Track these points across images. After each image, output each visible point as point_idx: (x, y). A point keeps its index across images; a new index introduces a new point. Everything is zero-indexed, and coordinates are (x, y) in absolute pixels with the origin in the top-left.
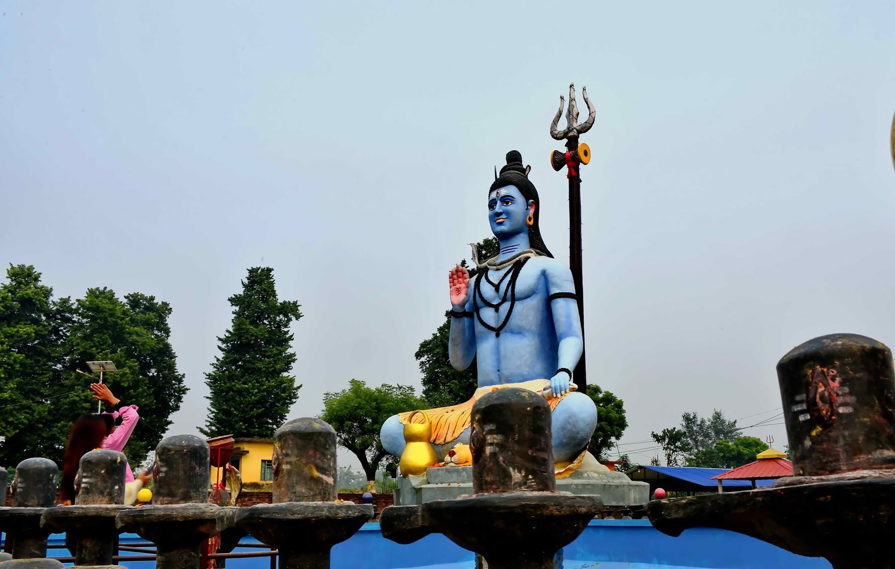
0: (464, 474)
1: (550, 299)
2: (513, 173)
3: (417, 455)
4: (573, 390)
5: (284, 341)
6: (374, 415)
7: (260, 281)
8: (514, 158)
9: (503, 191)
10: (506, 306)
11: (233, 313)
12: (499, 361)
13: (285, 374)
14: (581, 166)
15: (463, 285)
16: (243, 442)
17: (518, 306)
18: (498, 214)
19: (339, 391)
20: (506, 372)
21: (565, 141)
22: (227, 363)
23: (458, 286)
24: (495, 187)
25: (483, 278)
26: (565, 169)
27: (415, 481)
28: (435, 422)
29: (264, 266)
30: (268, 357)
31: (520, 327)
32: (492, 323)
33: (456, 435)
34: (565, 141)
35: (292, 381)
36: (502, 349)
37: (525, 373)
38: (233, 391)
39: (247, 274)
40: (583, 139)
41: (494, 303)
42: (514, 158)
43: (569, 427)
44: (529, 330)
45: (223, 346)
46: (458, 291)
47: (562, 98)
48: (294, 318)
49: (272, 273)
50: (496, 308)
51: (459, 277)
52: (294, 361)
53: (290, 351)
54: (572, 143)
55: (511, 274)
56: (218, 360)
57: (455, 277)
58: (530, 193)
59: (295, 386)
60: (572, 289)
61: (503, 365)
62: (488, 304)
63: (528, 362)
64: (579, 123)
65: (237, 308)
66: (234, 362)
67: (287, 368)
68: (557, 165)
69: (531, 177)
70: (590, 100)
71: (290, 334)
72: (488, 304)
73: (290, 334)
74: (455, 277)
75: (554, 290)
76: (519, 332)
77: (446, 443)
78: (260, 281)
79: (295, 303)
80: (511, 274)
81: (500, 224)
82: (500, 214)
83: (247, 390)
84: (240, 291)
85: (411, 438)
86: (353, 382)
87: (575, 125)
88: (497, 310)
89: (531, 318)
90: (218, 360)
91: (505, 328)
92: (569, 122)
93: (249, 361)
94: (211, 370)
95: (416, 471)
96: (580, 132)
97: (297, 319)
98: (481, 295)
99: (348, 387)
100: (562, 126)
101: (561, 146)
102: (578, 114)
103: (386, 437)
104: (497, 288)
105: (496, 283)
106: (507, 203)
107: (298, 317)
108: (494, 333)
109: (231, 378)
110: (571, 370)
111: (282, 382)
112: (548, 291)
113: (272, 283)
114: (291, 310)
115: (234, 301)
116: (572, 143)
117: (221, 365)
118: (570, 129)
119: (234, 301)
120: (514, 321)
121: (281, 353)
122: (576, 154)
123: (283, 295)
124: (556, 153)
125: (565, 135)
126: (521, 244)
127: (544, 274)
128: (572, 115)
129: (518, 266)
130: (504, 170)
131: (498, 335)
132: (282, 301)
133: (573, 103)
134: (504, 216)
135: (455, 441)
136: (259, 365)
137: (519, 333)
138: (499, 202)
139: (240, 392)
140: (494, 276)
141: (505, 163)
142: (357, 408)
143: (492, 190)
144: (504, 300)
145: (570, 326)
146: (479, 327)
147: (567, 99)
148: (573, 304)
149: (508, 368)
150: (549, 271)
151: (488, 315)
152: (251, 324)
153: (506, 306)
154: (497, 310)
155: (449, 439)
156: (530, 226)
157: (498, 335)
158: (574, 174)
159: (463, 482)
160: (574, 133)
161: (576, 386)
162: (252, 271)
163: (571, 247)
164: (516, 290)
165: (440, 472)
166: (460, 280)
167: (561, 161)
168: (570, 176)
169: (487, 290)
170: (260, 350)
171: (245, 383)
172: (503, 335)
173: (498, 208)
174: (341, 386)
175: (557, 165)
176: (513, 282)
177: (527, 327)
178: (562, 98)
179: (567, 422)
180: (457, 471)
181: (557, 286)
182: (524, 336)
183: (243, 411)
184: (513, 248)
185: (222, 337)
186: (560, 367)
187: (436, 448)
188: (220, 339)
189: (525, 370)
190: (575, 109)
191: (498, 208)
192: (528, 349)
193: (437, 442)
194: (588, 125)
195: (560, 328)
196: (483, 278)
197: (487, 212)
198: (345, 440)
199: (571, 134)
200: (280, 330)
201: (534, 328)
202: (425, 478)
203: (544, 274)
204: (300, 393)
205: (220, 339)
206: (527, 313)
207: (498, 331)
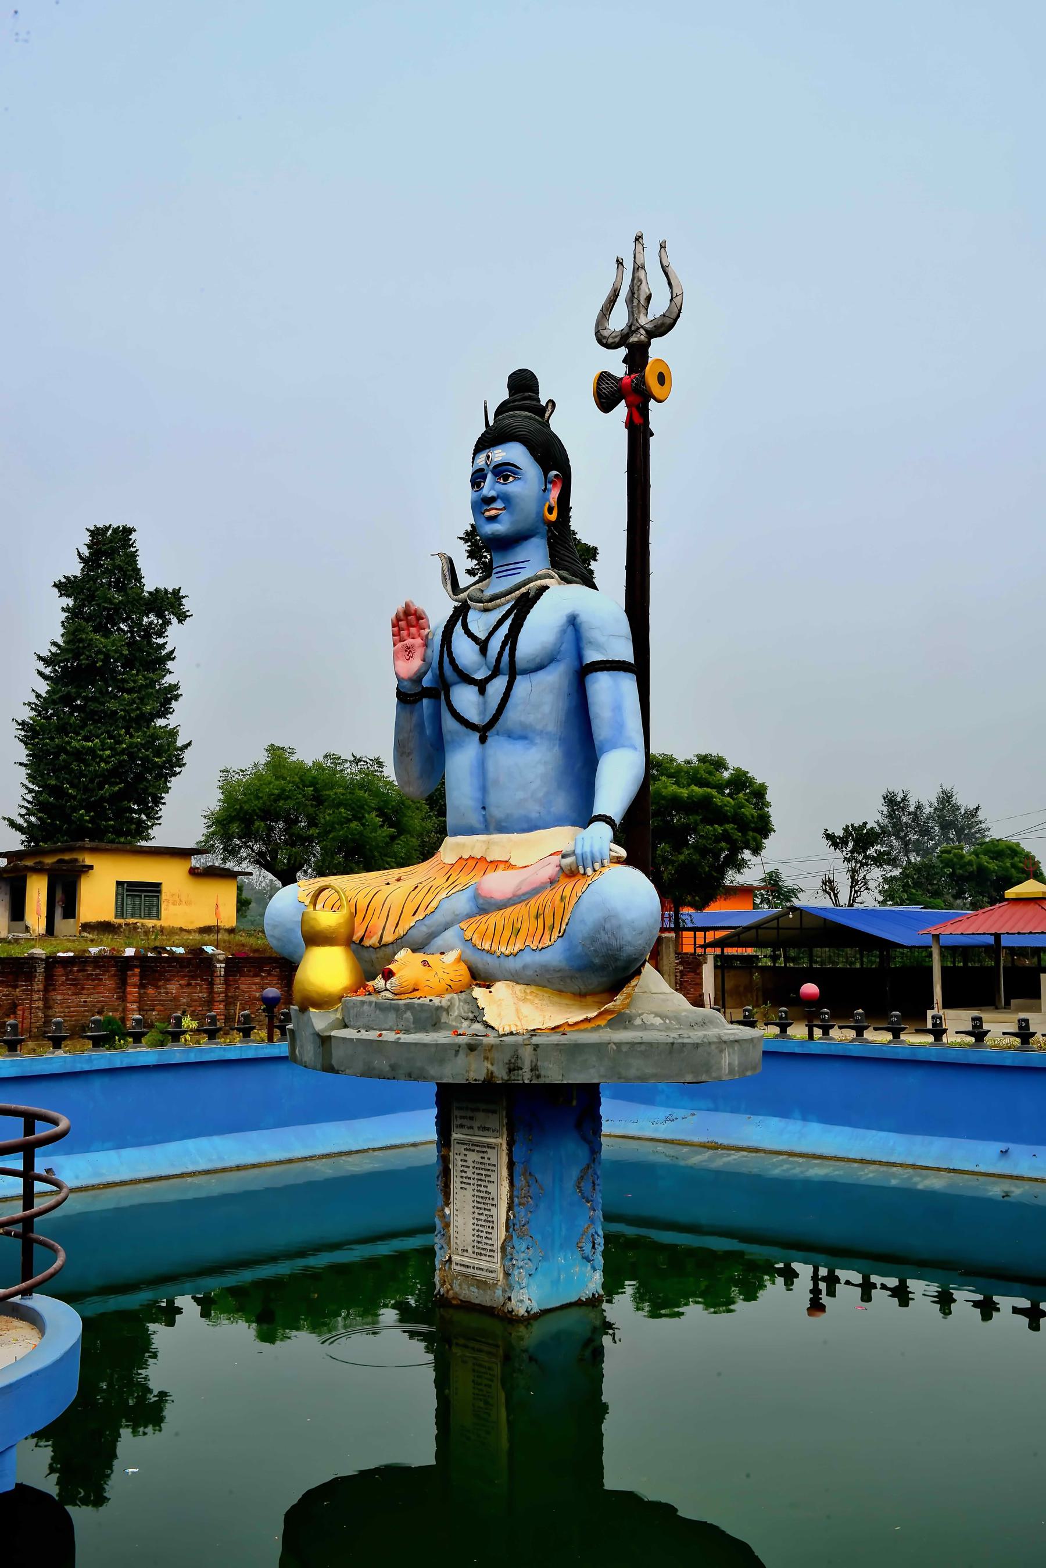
0: (409, 1015)
1: (584, 671)
2: (521, 417)
3: (326, 970)
4: (618, 861)
5: (157, 661)
6: (311, 810)
7: (111, 551)
8: (523, 384)
9: (499, 454)
11: (63, 609)
12: (484, 789)
13: (160, 722)
14: (652, 403)
15: (418, 641)
16: (83, 849)
17: (522, 685)
18: (489, 501)
19: (247, 764)
21: (623, 351)
22: (54, 702)
23: (409, 641)
24: (484, 444)
25: (459, 624)
26: (621, 410)
27: (320, 1021)
28: (363, 903)
29: (117, 522)
30: (129, 691)
31: (524, 726)
32: (473, 716)
33: (401, 931)
34: (623, 351)
35: (173, 734)
37: (534, 815)
38: (66, 752)
39: (87, 538)
40: (657, 348)
41: (479, 676)
42: (523, 384)
43: (604, 937)
44: (541, 733)
45: (47, 671)
46: (409, 651)
47: (620, 263)
48: (174, 620)
49: (133, 537)
50: (482, 686)
51: (409, 625)
52: (176, 698)
53: (168, 680)
54: (637, 358)
55: (509, 621)
56: (38, 696)
57: (402, 624)
58: (552, 458)
59: (180, 743)
60: (625, 652)
61: (493, 798)
62: (467, 679)
63: (541, 794)
64: (650, 317)
65: (70, 602)
66: (67, 700)
67: (164, 713)
68: (606, 401)
69: (557, 424)
70: (673, 269)
71: (169, 648)
72: (467, 679)
73: (169, 648)
74: (402, 624)
75: (592, 656)
76: (522, 735)
77: (382, 946)
78: (111, 551)
79: (176, 592)
80: (509, 621)
81: (493, 519)
82: (493, 500)
83: (92, 751)
84: (75, 569)
85: (315, 938)
86: (272, 749)
87: (643, 320)
88: (482, 691)
89: (546, 709)
90: (38, 696)
91: (497, 726)
92: (631, 313)
93: (94, 699)
94: (27, 714)
95: (323, 1002)
97: (180, 621)
98: (452, 661)
99: (263, 758)
100: (619, 320)
101: (615, 363)
102: (649, 298)
103: (275, 927)
104: (483, 646)
105: (482, 636)
106: (506, 478)
107: (182, 617)
109: (63, 729)
110: (617, 818)
111: (155, 737)
112: (580, 656)
113: (134, 555)
114: (169, 604)
115: (65, 587)
116: (637, 358)
117: (43, 705)
118: (632, 328)
119: (65, 587)
120: (513, 715)
121: (152, 683)
122: (642, 380)
123: (154, 576)
124: (604, 377)
125: (623, 340)
126: (533, 559)
127: (573, 621)
128: (638, 301)
129: (525, 604)
130: (502, 409)
131: (483, 740)
132: (152, 590)
133: (641, 274)
134: (499, 504)
135: (400, 943)
136: (112, 705)
137: (523, 737)
138: (490, 476)
139: (78, 755)
140: (479, 622)
141: (505, 395)
142: (279, 797)
143: (477, 450)
144: (496, 672)
145: (619, 726)
146: (449, 723)
147: (629, 265)
148: (628, 684)
149: (503, 803)
150: (583, 618)
152: (96, 630)
153: (498, 685)
154: (482, 691)
155: (388, 938)
156: (550, 524)
157: (483, 740)
158: (638, 420)
159: (407, 1031)
160: (641, 336)
161: (623, 853)
162: (96, 533)
163: (628, 568)
164: (517, 653)
165: (366, 1007)
166: (413, 630)
167: (613, 394)
168: (630, 424)
169: (464, 650)
170: (114, 679)
171: (87, 739)
173: (489, 488)
174: (248, 757)
175: (606, 401)
176: (512, 637)
177: (539, 727)
178: (620, 263)
179: (600, 927)
180: (396, 1009)
181: (599, 647)
182: (532, 743)
183: (86, 790)
184: (516, 568)
185: (45, 654)
186: (596, 813)
187: (365, 954)
188: (40, 658)
189: (534, 810)
190: (643, 286)
191: (489, 488)
192: (541, 769)
193: (367, 942)
194: (669, 321)
195: (601, 730)
196: (459, 624)
197: (467, 493)
198: (260, 854)
199: (633, 339)
200: (150, 643)
201: (551, 728)
202: (339, 1015)
203: (573, 621)
204: (187, 756)
205: (40, 658)
206: (539, 698)
207: (483, 732)
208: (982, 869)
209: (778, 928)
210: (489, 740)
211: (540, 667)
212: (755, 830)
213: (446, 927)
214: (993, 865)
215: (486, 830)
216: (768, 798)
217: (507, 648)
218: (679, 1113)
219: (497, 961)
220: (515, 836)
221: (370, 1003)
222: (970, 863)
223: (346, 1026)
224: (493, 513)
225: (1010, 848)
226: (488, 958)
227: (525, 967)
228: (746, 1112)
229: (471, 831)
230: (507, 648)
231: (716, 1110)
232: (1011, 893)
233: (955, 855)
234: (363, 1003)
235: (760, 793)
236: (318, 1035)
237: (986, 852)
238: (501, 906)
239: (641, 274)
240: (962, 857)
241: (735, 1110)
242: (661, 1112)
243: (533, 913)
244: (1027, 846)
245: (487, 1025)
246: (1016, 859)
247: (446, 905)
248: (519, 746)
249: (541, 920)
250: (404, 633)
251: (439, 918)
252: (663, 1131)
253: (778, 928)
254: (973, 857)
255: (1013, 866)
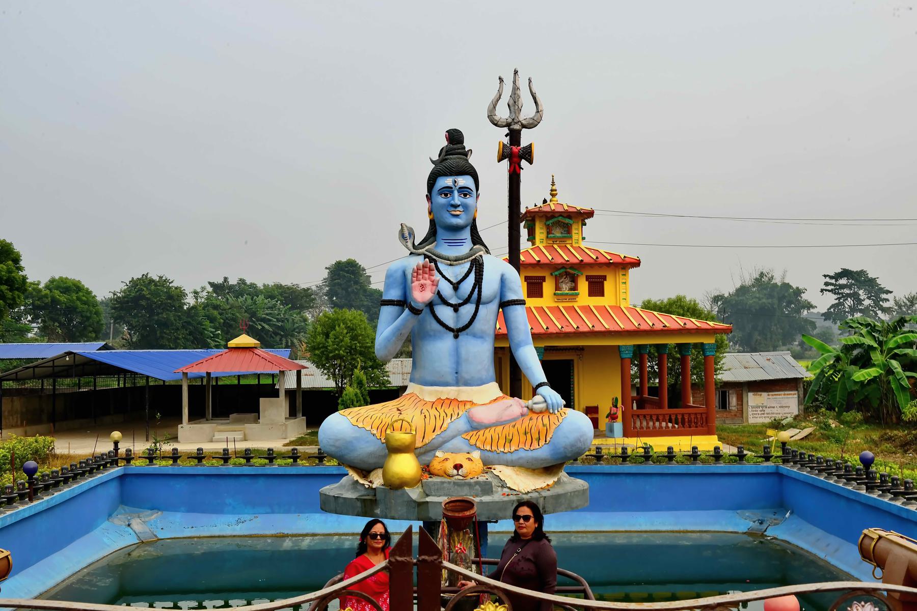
8: (455, 137)
10: (468, 309)
12: (458, 363)
20: (465, 375)
21: (506, 130)
23: (422, 282)
32: (451, 324)
36: (463, 352)
41: (453, 301)
42: (455, 137)
43: (579, 445)
51: (424, 273)
62: (445, 302)
72: (445, 302)
75: (511, 296)
81: (457, 216)
82: (456, 206)
91: (468, 331)
96: (524, 126)
100: (503, 113)
104: (456, 286)
106: (465, 195)
108: (451, 335)
120: (477, 325)
131: (456, 337)
133: (518, 92)
134: (460, 209)
144: (467, 301)
149: (468, 371)
151: (445, 313)
157: (456, 337)
160: (517, 127)
164: (483, 294)
166: (427, 276)
172: (462, 336)
181: (515, 292)
207: (457, 333)
208: (55, 301)
209: (53, 366)
210: (460, 337)
211: (491, 301)
212: (18, 289)
213: (453, 437)
214: (63, 298)
215: (457, 383)
216: (22, 264)
217: (476, 290)
218: (244, 517)
219: (496, 456)
220: (474, 388)
221: (449, 483)
222: (46, 296)
223: (427, 495)
224: (458, 213)
225: (74, 285)
226: (490, 454)
227: (520, 458)
228: (295, 512)
229: (446, 384)
230: (476, 290)
231: (273, 512)
232: (233, 343)
233: (34, 289)
234: (443, 483)
235: (16, 260)
236: (415, 501)
237: (57, 288)
238: (487, 427)
239: (518, 92)
240: (40, 291)
241: (288, 511)
242: (232, 518)
243: (522, 431)
244: (87, 284)
245: (509, 488)
246: (81, 294)
247: (453, 426)
248: (479, 341)
249: (529, 436)
250: (420, 277)
251: (449, 433)
252: (239, 530)
253: (53, 366)
254: (48, 292)
255: (78, 299)
